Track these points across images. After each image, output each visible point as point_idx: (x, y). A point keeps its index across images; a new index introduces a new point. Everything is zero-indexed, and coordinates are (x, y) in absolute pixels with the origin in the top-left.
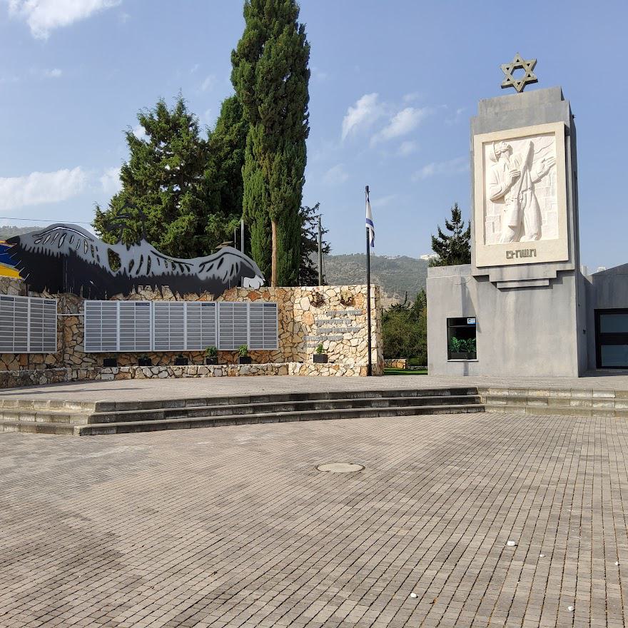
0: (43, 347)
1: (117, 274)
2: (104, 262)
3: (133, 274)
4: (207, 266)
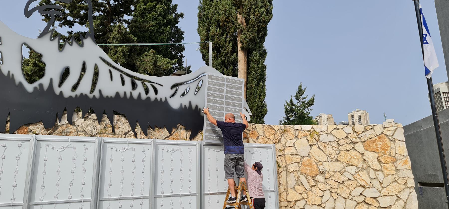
1: (35, 88)
3: (66, 90)
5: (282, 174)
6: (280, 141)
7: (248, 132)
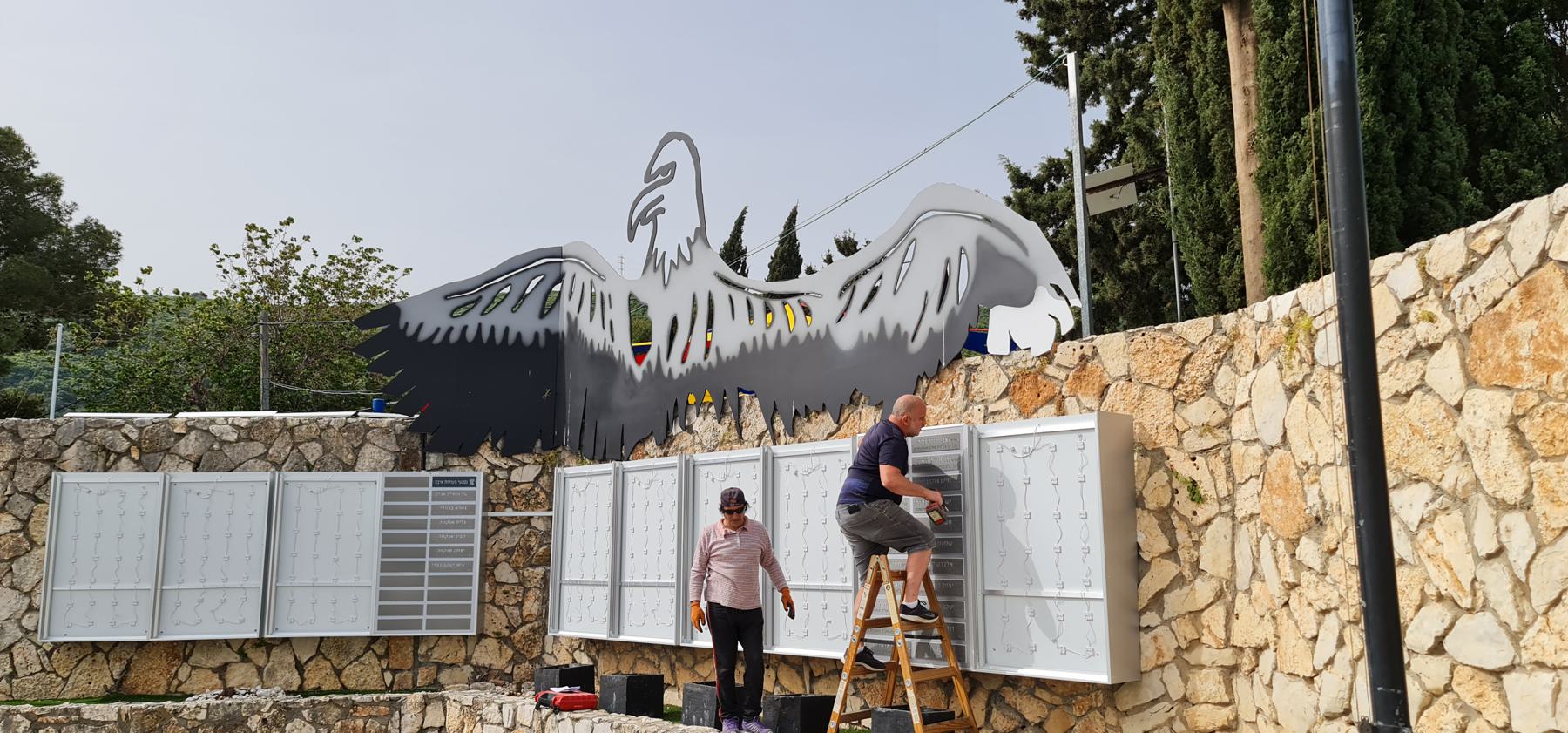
0: (425, 617)
4: (863, 288)
5: (1210, 532)
6: (1209, 386)
7: (1062, 375)
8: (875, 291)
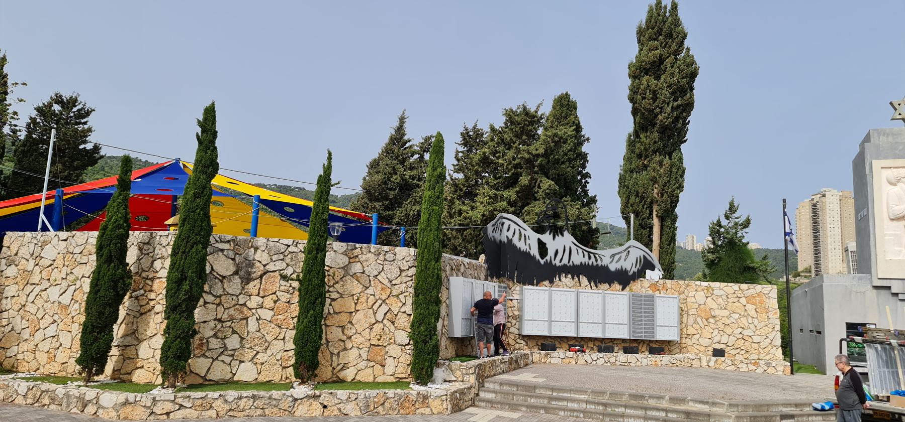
2: (535, 252)
8: (619, 259)
